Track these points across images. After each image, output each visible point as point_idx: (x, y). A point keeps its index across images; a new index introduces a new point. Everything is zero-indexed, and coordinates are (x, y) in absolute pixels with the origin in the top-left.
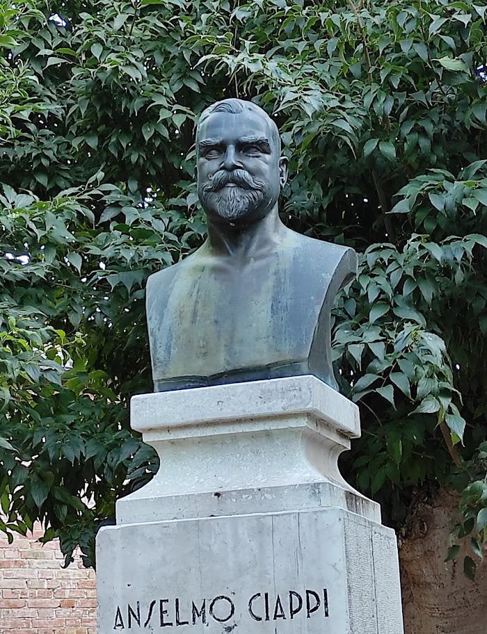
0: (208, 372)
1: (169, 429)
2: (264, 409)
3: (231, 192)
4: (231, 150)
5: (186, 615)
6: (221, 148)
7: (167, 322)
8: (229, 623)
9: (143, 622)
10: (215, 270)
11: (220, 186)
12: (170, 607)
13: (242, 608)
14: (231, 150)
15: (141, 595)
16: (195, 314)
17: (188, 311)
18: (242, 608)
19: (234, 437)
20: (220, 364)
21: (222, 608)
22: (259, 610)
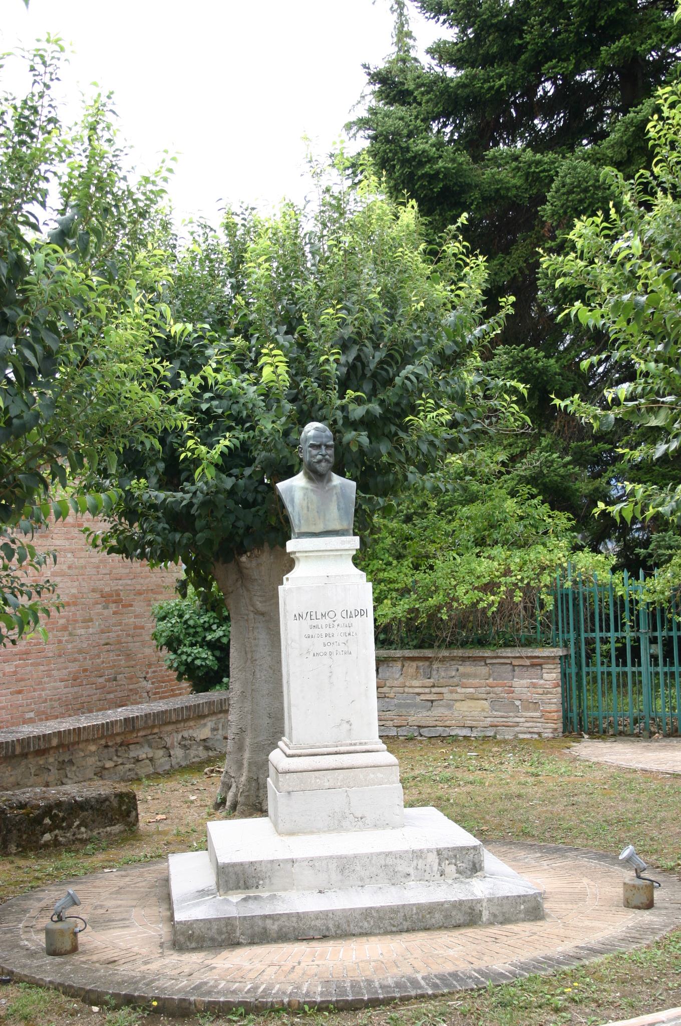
0: (317, 531)
1: (306, 552)
4: (323, 447)
5: (319, 616)
6: (318, 447)
7: (297, 509)
11: (320, 462)
13: (339, 615)
14: (323, 447)
16: (308, 508)
17: (305, 504)
18: (339, 615)
20: (320, 528)
22: (344, 615)
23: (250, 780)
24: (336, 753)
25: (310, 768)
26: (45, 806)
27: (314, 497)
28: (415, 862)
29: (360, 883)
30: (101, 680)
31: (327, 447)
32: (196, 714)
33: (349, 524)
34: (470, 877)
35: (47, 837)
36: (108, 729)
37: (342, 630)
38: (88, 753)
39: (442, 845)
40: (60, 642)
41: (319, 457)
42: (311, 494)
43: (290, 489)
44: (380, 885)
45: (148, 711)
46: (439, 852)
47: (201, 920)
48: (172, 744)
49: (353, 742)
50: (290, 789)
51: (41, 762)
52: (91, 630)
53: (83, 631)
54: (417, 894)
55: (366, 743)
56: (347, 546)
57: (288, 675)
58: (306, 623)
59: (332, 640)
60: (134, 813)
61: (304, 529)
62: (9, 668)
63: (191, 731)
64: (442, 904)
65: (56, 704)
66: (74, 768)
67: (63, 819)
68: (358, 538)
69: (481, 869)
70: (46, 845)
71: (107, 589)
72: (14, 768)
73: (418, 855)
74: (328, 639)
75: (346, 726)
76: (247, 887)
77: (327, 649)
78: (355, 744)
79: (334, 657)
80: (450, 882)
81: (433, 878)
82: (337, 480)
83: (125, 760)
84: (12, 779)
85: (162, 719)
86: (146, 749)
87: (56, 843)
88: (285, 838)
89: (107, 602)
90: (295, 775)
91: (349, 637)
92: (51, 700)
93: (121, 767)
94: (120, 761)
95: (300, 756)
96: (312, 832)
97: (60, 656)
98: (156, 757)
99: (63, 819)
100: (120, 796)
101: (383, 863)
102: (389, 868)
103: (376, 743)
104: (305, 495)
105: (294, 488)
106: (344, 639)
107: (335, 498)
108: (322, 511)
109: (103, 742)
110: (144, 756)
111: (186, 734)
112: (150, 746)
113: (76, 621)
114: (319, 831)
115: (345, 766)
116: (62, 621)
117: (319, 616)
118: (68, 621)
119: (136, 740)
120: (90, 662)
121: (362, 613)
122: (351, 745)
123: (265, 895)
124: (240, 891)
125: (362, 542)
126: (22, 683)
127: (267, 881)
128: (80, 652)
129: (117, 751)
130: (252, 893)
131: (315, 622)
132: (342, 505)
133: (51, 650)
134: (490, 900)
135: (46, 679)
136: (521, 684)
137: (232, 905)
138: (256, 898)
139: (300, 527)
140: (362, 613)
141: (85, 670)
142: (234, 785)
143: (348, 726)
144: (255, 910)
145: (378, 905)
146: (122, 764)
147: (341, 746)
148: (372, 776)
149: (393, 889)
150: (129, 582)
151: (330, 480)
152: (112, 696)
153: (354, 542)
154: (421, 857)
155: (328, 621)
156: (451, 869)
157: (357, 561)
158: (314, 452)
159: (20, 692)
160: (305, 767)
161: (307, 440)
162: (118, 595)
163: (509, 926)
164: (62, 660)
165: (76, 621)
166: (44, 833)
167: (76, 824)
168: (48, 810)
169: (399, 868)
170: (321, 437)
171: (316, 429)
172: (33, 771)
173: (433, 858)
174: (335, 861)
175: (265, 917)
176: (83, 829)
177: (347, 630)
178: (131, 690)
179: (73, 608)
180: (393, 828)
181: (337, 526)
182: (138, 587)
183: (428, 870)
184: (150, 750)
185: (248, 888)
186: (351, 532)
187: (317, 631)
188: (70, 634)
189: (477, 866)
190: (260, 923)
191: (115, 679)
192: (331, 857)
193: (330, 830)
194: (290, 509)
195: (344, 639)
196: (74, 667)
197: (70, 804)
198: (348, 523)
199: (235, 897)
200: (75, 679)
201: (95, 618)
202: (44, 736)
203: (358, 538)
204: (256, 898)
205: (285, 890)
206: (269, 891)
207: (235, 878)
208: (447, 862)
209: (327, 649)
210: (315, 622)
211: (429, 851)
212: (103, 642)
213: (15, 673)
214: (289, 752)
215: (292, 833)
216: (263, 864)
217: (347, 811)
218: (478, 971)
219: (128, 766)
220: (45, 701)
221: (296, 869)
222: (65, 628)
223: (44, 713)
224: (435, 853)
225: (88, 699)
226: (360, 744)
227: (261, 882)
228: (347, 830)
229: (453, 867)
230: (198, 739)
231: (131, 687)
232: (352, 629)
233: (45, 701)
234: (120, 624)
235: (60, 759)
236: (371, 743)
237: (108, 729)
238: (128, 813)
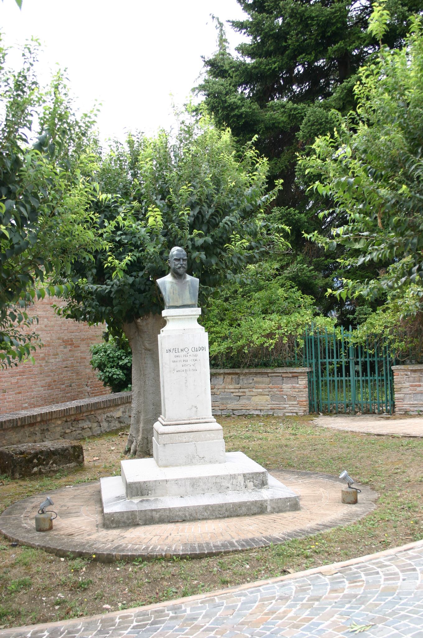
0: (178, 305)
2: (192, 314)
4: (181, 260)
6: (179, 260)
7: (167, 293)
11: (179, 268)
12: (177, 349)
14: (181, 260)
15: (171, 348)
17: (172, 291)
20: (180, 303)
21: (186, 350)
23: (143, 438)
24: (189, 424)
26: (34, 453)
27: (176, 287)
28: (232, 481)
29: (202, 492)
31: (184, 260)
32: (114, 404)
33: (195, 301)
34: (261, 488)
35: (35, 469)
36: (67, 412)
39: (246, 472)
40: (41, 366)
41: (179, 265)
42: (175, 285)
43: (164, 283)
45: (89, 402)
46: (244, 475)
48: (102, 419)
50: (165, 443)
51: (32, 430)
52: (57, 360)
53: (53, 361)
54: (233, 498)
56: (194, 313)
57: (163, 382)
58: (173, 354)
60: (81, 457)
61: (171, 304)
62: (14, 380)
63: (111, 413)
64: (246, 503)
65: (39, 399)
66: (49, 433)
67: (44, 460)
68: (200, 309)
69: (267, 484)
70: (35, 474)
71: (66, 338)
72: (17, 433)
73: (233, 477)
75: (194, 409)
76: (142, 495)
77: (184, 368)
78: (199, 419)
79: (188, 372)
80: (250, 491)
82: (189, 278)
83: (76, 429)
84: (16, 439)
85: (96, 407)
86: (88, 423)
87: (40, 472)
88: (162, 469)
89: (66, 345)
90: (167, 435)
92: (37, 397)
93: (74, 432)
94: (74, 429)
96: (177, 466)
98: (93, 427)
99: (44, 460)
100: (74, 447)
101: (215, 481)
102: (217, 484)
103: (211, 418)
105: (166, 282)
107: (188, 287)
108: (181, 295)
109: (65, 419)
110: (87, 426)
111: (109, 415)
112: (90, 421)
113: (49, 355)
116: (42, 355)
119: (82, 418)
121: (203, 349)
122: (197, 419)
125: (202, 311)
126: (21, 388)
127: (153, 491)
128: (52, 371)
129: (72, 424)
130: (145, 498)
131: (177, 354)
132: (192, 291)
133: (36, 370)
134: (271, 500)
135: (34, 386)
136: (287, 387)
137: (135, 504)
138: (147, 500)
139: (169, 303)
140: (203, 349)
141: (55, 381)
142: (135, 441)
143: (195, 409)
144: (147, 506)
145: (212, 503)
147: (192, 420)
149: (220, 495)
150: (78, 334)
151: (185, 278)
152: (69, 395)
153: (198, 311)
154: (235, 478)
155: (184, 353)
157: (199, 321)
158: (177, 263)
159: (20, 393)
160: (173, 431)
161: (172, 256)
162: (72, 341)
163: (281, 514)
164: (42, 376)
165: (49, 355)
166: (34, 467)
167: (51, 462)
168: (36, 455)
169: (223, 484)
170: (180, 255)
171: (178, 250)
172: (27, 435)
173: (241, 479)
175: (152, 510)
176: (54, 465)
177: (195, 358)
179: (48, 348)
181: (188, 302)
182: (83, 337)
184: (89, 423)
185: (143, 495)
187: (178, 359)
188: (46, 362)
190: (149, 513)
191: (71, 386)
192: (187, 479)
193: (186, 464)
194: (164, 293)
195: (193, 363)
196: (48, 380)
197: (47, 452)
198: (195, 301)
199: (136, 500)
200: (49, 386)
201: (59, 353)
202: (33, 416)
203: (200, 309)
204: (147, 500)
205: (163, 496)
207: (136, 490)
209: (184, 368)
210: (177, 354)
211: (239, 475)
212: (64, 366)
213: (17, 383)
214: (164, 423)
215: (166, 466)
217: (195, 454)
218: (265, 538)
219: (78, 432)
220: (33, 398)
221: (168, 485)
222: (43, 359)
223: (33, 404)
225: (56, 396)
226: (202, 418)
227: (150, 492)
228: (195, 464)
229: (252, 483)
230: (115, 417)
231: (79, 390)
232: (197, 358)
233: (33, 398)
234: (73, 357)
235: (42, 429)
237: (67, 412)
238: (78, 456)
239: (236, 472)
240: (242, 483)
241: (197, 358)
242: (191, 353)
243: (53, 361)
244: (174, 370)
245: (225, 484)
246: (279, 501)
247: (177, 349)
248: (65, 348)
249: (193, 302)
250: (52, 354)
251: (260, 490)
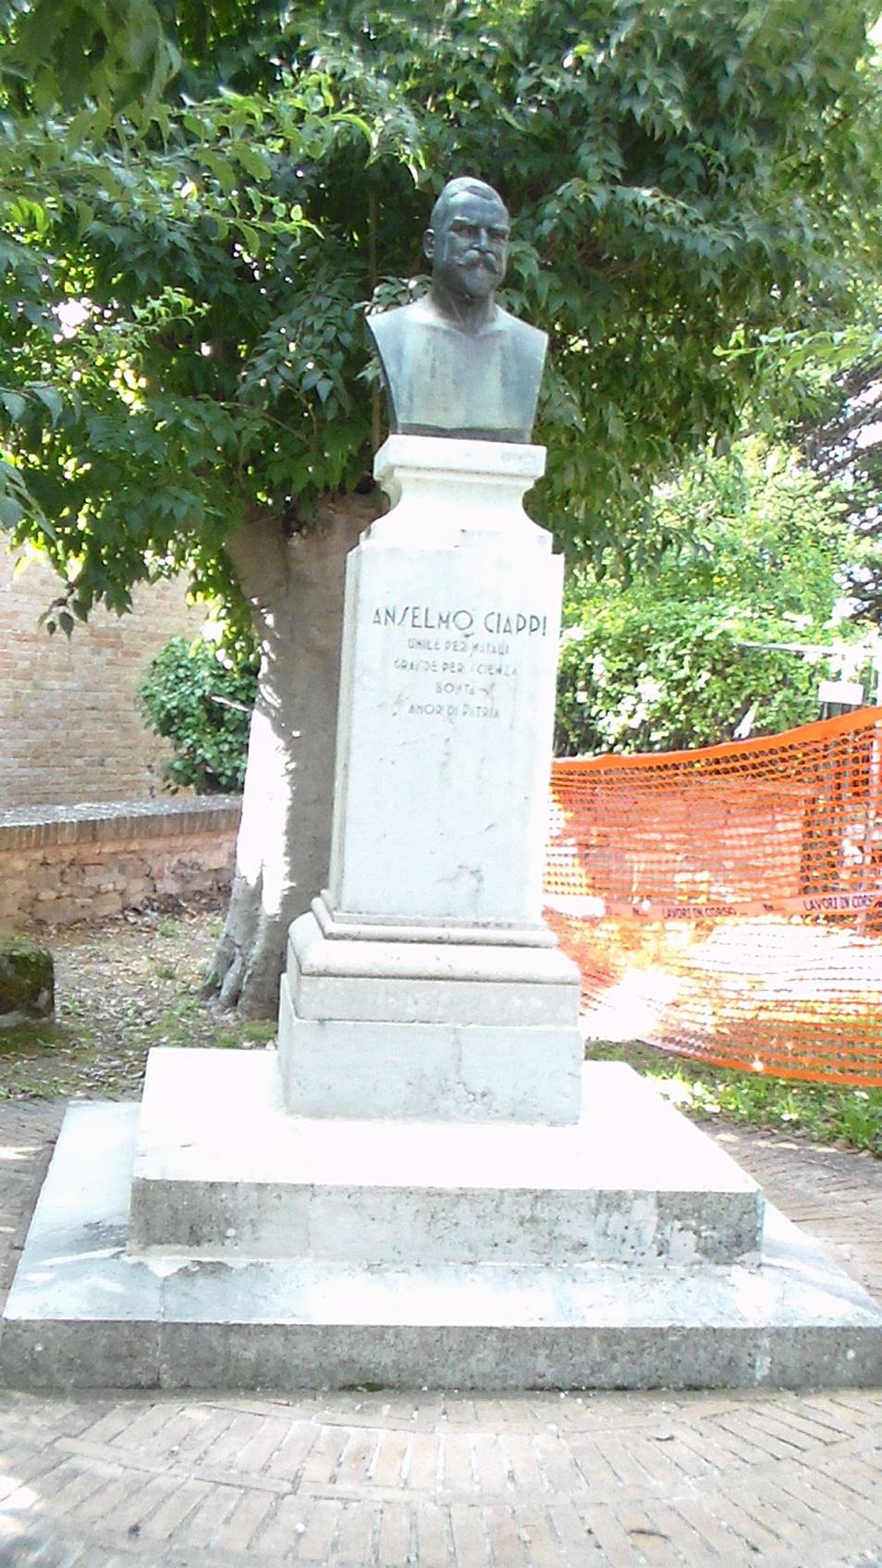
1: (418, 469)
3: (481, 272)
4: (483, 233)
5: (434, 621)
6: (473, 231)
7: (407, 370)
8: (468, 631)
9: (398, 620)
10: (446, 332)
11: (472, 264)
12: (421, 613)
13: (479, 622)
14: (483, 233)
16: (433, 370)
17: (426, 361)
18: (479, 622)
19: (470, 485)
21: (463, 620)
22: (492, 624)
23: (266, 956)
24: (440, 941)
25: (377, 971)
27: (449, 348)
28: (602, 1217)
29: (469, 1256)
30: (78, 762)
31: (494, 234)
32: (188, 824)
33: (524, 421)
36: (47, 836)
37: (480, 658)
38: (8, 871)
40: (17, 696)
43: (398, 331)
44: (514, 1265)
45: (125, 812)
46: (662, 1201)
47: (67, 1322)
48: (161, 870)
49: (485, 921)
52: (69, 685)
53: (55, 684)
55: (510, 926)
56: (514, 467)
57: (348, 749)
58: (401, 633)
59: (455, 679)
60: (46, 994)
61: (419, 418)
64: (660, 1333)
68: (542, 450)
69: (754, 1245)
73: (612, 1202)
74: (447, 677)
75: (468, 882)
76: (195, 1239)
77: (445, 699)
78: (485, 926)
80: (680, 1270)
81: (640, 1259)
82: (504, 320)
85: (145, 827)
88: (304, 1123)
89: (99, 644)
90: (339, 982)
91: (497, 677)
95: (355, 939)
96: (364, 1115)
97: (16, 718)
100: (21, 963)
102: (540, 1224)
103: (535, 927)
104: (429, 342)
105: (406, 327)
106: (483, 681)
107: (497, 357)
109: (39, 855)
110: (110, 886)
111: (186, 858)
112: (122, 870)
114: (383, 1114)
115: (458, 974)
116: (25, 664)
117: (434, 621)
118: (33, 664)
120: (63, 733)
121: (534, 624)
122: (476, 924)
123: (238, 1262)
124: (179, 1247)
125: (552, 468)
127: (247, 1229)
128: (49, 714)
129: (62, 873)
130: (206, 1254)
131: (422, 634)
132: (512, 375)
134: (778, 1334)
136: (739, 835)
137: (152, 1287)
138: (217, 1269)
140: (534, 624)
141: (55, 744)
142: (238, 960)
143: (473, 882)
146: (70, 896)
147: (454, 925)
148: (517, 1002)
149: (547, 1279)
152: (94, 787)
154: (618, 1207)
155: (453, 634)
156: (684, 1243)
158: (463, 242)
161: (449, 211)
162: (119, 636)
163: (821, 1402)
164: (18, 724)
165: (46, 667)
169: (562, 1229)
170: (482, 208)
171: (472, 190)
173: (645, 1213)
174: (413, 1199)
175: (229, 1329)
177: (496, 660)
178: (125, 783)
180: (552, 1124)
181: (496, 420)
182: (151, 628)
183: (632, 1240)
185: (198, 1243)
186: (528, 436)
187: (425, 655)
188: (36, 686)
189: (745, 1239)
192: (406, 1192)
193: (408, 1111)
195: (483, 681)
196: (36, 738)
199: (165, 1263)
200: (37, 756)
203: (542, 450)
204: (217, 1269)
205: (289, 1255)
206: (248, 1253)
207: (174, 1215)
208: (678, 1224)
209: (445, 699)
210: (422, 634)
211: (637, 1195)
214: (332, 927)
215: (318, 1113)
216: (240, 1189)
222: (27, 676)
224: (652, 1202)
225: (56, 789)
226: (498, 925)
228: (447, 1117)
230: (205, 868)
231: (125, 778)
232: (508, 660)
234: (117, 681)
236: (523, 927)
237: (47, 836)
238: (35, 995)
239: (627, 1185)
240: (649, 1232)
241: (508, 660)
242: (480, 636)
243: (55, 684)
244: (399, 702)
245: (579, 1228)
246: (810, 1339)
247: (421, 613)
248: (97, 652)
249: (512, 421)
250: (53, 663)
251: (722, 1270)
